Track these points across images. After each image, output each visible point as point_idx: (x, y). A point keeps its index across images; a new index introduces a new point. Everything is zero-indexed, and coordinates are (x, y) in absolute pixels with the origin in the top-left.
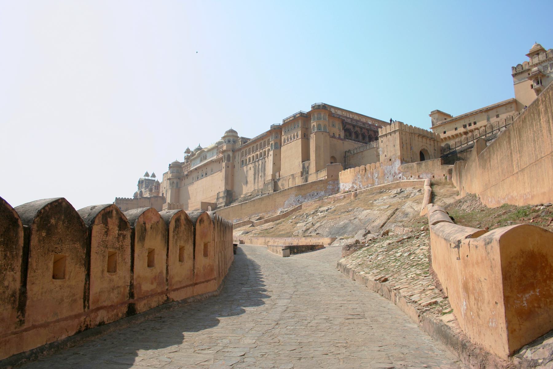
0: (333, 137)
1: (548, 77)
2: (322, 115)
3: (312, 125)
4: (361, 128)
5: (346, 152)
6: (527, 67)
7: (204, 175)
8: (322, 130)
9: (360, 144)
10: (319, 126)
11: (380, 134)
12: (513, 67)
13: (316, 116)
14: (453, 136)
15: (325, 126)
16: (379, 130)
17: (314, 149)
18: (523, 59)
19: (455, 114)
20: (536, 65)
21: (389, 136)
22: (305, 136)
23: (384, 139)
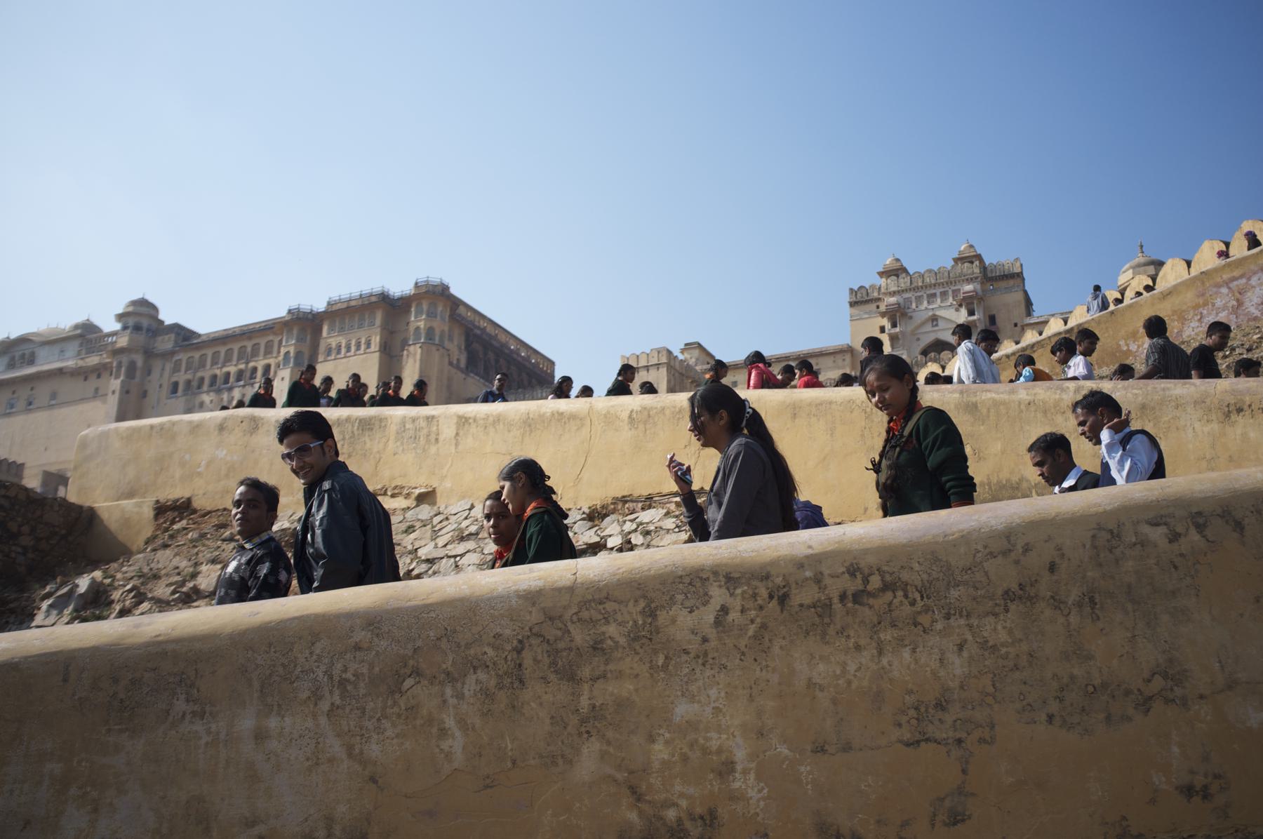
1: (911, 318)
2: (440, 309)
6: (876, 294)
7: (21, 404)
10: (430, 332)
13: (425, 307)
18: (870, 279)
20: (893, 294)
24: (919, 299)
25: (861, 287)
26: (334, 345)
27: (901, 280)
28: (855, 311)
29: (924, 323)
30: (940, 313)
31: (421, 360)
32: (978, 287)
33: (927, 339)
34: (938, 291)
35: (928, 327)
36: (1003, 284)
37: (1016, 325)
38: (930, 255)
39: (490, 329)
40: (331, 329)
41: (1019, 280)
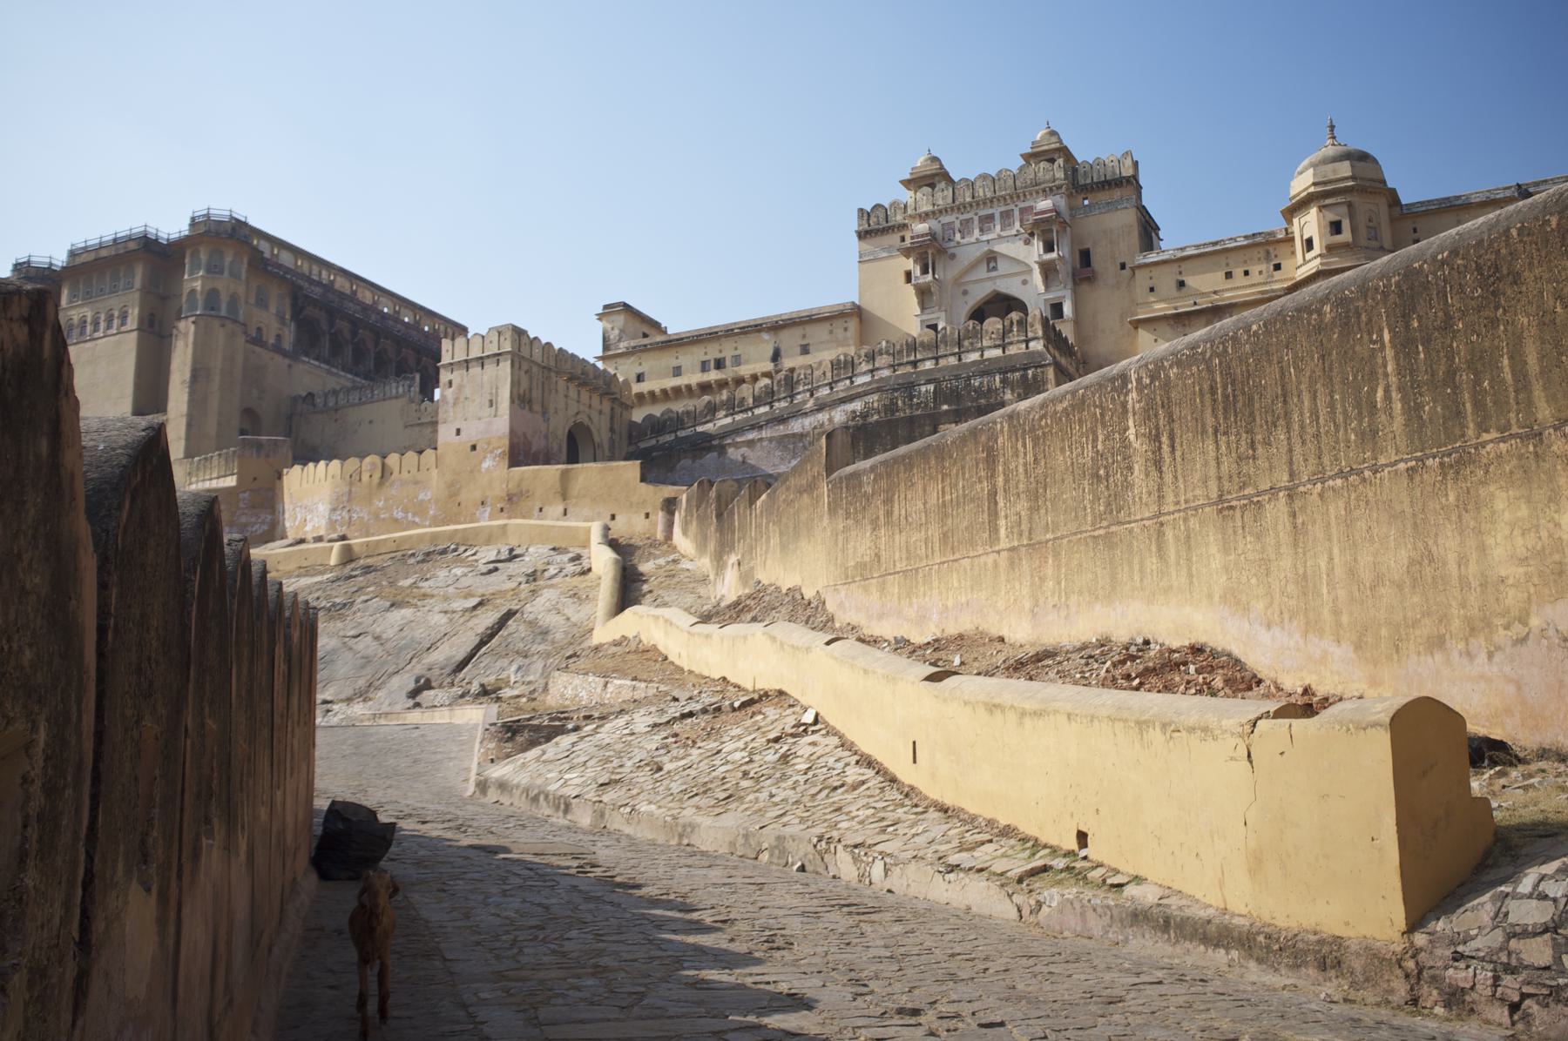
0: (257, 340)
1: (953, 256)
2: (228, 259)
3: (187, 288)
4: (355, 324)
5: (295, 399)
6: (899, 218)
8: (223, 313)
9: (345, 379)
10: (212, 297)
11: (446, 359)
12: (861, 210)
13: (203, 257)
14: (664, 391)
15: (233, 300)
16: (446, 344)
17: (187, 376)
18: (891, 192)
19: (676, 324)
20: (924, 217)
21: (475, 370)
22: (151, 324)
23: (456, 376)
24: (966, 227)
25: (877, 206)
26: (76, 319)
27: (939, 195)
28: (867, 246)
29: (973, 266)
30: (1001, 248)
31: (195, 344)
32: (1062, 202)
33: (979, 293)
34: (997, 211)
35: (982, 272)
36: (1103, 197)
37: (1123, 266)
38: (984, 152)
39: (341, 284)
40: (73, 296)
41: (1127, 191)
